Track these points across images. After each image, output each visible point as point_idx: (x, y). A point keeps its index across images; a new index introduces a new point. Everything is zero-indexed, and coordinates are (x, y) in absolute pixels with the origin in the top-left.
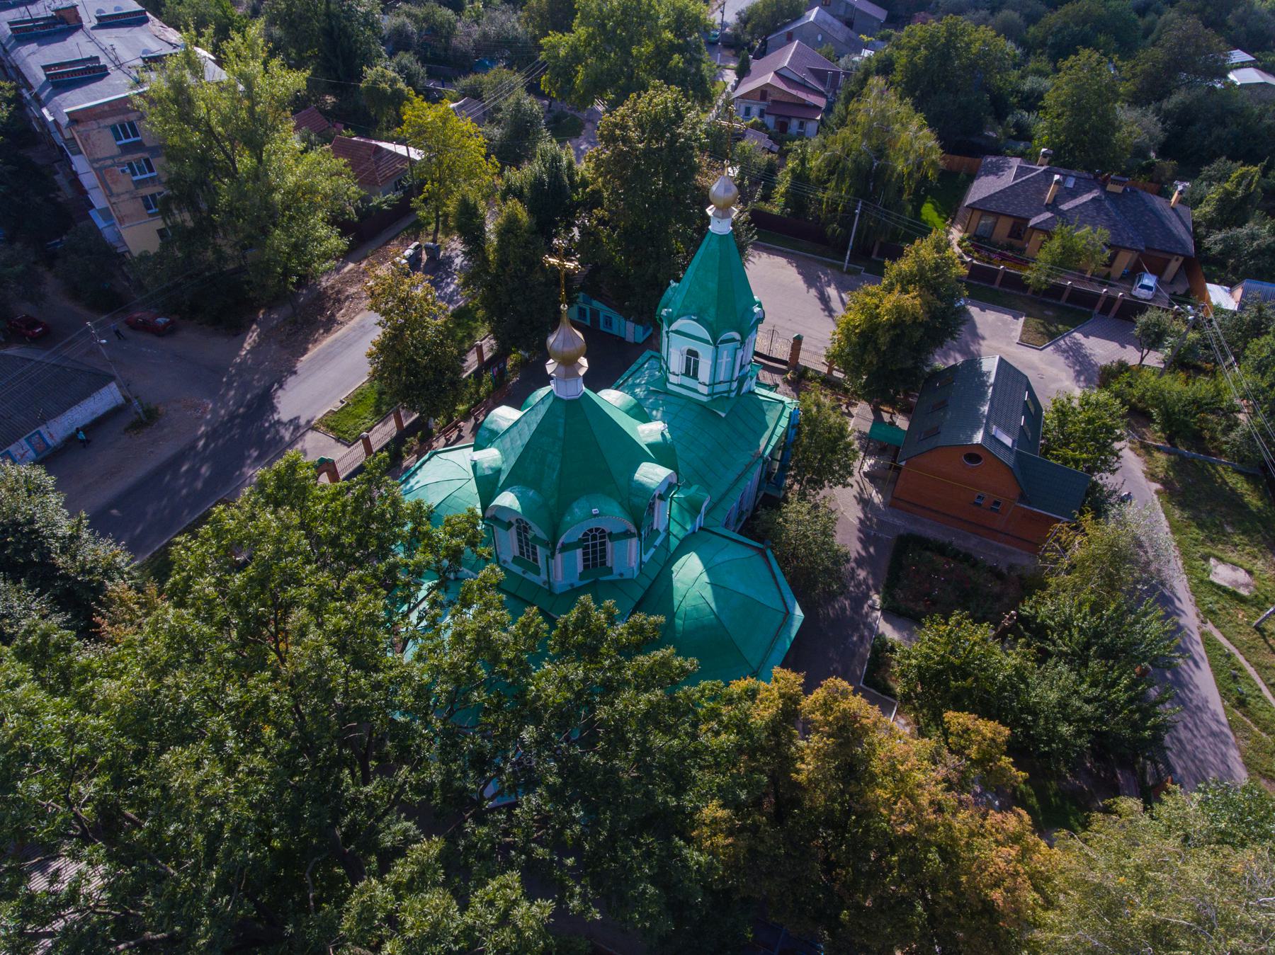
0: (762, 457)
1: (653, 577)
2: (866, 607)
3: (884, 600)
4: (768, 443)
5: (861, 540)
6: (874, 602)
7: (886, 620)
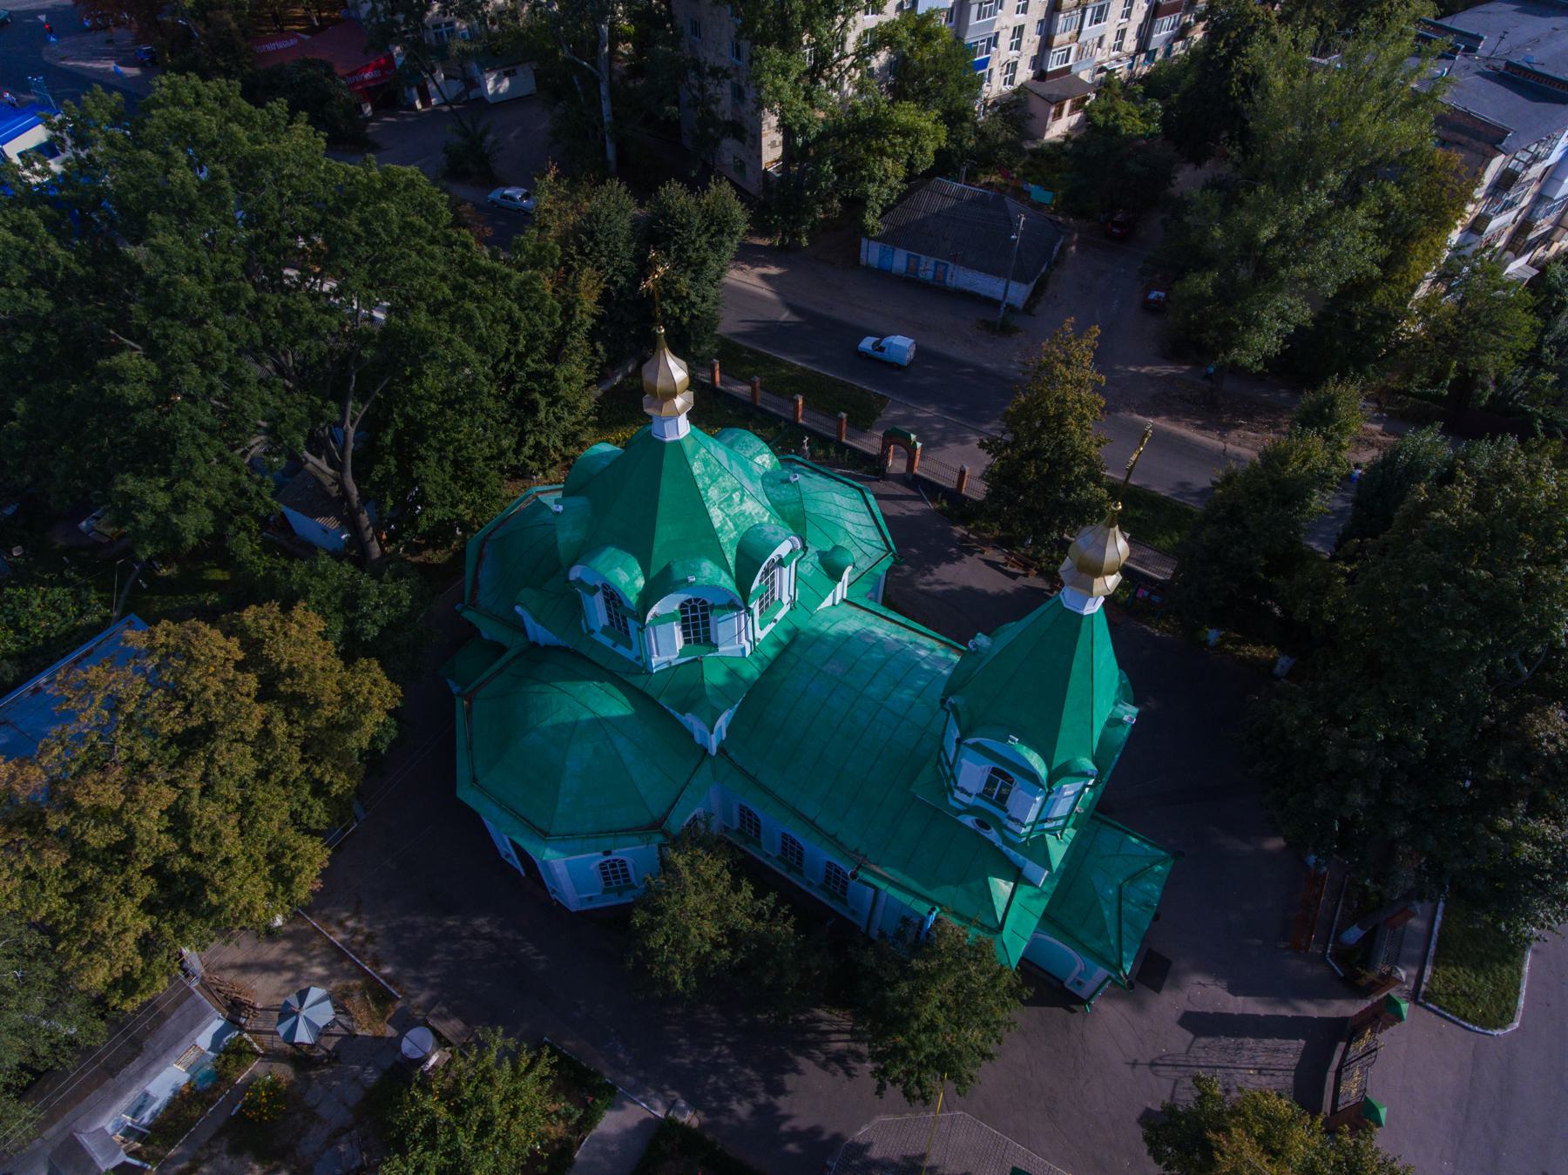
0: (859, 867)
1: (592, 656)
2: (676, 1094)
3: (685, 1130)
4: (892, 883)
5: (815, 1131)
6: (683, 1112)
7: (646, 1123)
